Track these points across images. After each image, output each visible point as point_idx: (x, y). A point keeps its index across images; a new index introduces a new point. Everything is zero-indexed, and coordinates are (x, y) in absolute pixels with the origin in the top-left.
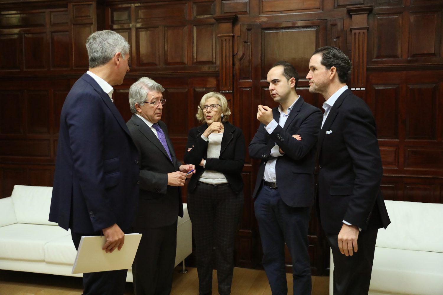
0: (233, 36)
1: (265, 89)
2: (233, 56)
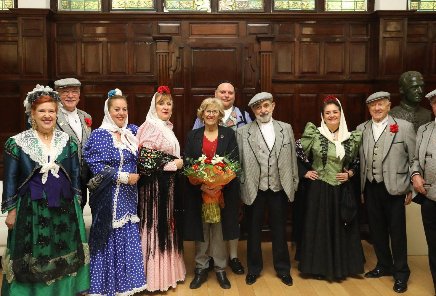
0: (169, 53)
2: (169, 68)
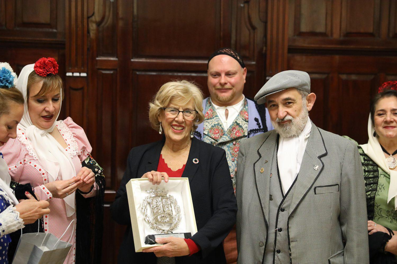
1: (138, 73)
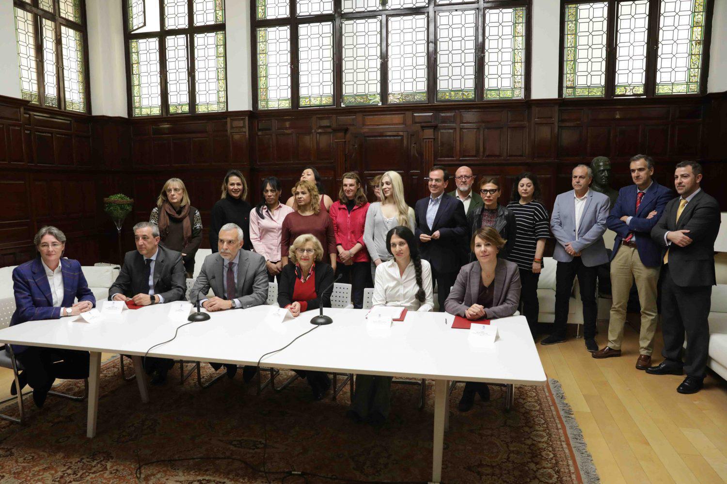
0: (345, 141)
